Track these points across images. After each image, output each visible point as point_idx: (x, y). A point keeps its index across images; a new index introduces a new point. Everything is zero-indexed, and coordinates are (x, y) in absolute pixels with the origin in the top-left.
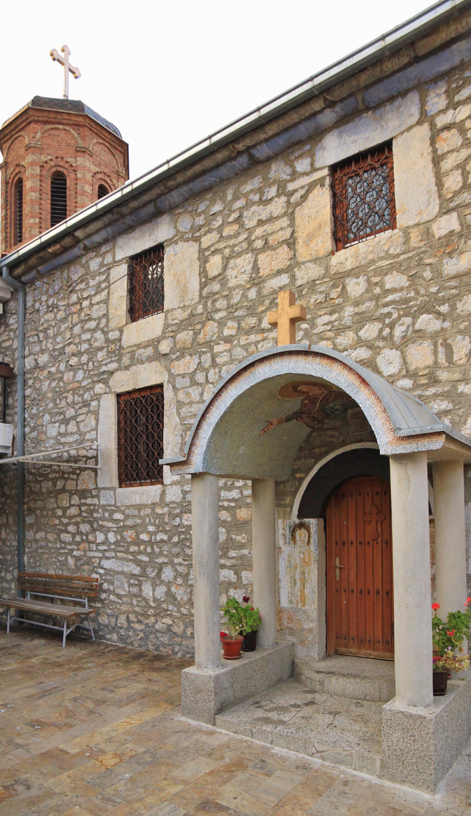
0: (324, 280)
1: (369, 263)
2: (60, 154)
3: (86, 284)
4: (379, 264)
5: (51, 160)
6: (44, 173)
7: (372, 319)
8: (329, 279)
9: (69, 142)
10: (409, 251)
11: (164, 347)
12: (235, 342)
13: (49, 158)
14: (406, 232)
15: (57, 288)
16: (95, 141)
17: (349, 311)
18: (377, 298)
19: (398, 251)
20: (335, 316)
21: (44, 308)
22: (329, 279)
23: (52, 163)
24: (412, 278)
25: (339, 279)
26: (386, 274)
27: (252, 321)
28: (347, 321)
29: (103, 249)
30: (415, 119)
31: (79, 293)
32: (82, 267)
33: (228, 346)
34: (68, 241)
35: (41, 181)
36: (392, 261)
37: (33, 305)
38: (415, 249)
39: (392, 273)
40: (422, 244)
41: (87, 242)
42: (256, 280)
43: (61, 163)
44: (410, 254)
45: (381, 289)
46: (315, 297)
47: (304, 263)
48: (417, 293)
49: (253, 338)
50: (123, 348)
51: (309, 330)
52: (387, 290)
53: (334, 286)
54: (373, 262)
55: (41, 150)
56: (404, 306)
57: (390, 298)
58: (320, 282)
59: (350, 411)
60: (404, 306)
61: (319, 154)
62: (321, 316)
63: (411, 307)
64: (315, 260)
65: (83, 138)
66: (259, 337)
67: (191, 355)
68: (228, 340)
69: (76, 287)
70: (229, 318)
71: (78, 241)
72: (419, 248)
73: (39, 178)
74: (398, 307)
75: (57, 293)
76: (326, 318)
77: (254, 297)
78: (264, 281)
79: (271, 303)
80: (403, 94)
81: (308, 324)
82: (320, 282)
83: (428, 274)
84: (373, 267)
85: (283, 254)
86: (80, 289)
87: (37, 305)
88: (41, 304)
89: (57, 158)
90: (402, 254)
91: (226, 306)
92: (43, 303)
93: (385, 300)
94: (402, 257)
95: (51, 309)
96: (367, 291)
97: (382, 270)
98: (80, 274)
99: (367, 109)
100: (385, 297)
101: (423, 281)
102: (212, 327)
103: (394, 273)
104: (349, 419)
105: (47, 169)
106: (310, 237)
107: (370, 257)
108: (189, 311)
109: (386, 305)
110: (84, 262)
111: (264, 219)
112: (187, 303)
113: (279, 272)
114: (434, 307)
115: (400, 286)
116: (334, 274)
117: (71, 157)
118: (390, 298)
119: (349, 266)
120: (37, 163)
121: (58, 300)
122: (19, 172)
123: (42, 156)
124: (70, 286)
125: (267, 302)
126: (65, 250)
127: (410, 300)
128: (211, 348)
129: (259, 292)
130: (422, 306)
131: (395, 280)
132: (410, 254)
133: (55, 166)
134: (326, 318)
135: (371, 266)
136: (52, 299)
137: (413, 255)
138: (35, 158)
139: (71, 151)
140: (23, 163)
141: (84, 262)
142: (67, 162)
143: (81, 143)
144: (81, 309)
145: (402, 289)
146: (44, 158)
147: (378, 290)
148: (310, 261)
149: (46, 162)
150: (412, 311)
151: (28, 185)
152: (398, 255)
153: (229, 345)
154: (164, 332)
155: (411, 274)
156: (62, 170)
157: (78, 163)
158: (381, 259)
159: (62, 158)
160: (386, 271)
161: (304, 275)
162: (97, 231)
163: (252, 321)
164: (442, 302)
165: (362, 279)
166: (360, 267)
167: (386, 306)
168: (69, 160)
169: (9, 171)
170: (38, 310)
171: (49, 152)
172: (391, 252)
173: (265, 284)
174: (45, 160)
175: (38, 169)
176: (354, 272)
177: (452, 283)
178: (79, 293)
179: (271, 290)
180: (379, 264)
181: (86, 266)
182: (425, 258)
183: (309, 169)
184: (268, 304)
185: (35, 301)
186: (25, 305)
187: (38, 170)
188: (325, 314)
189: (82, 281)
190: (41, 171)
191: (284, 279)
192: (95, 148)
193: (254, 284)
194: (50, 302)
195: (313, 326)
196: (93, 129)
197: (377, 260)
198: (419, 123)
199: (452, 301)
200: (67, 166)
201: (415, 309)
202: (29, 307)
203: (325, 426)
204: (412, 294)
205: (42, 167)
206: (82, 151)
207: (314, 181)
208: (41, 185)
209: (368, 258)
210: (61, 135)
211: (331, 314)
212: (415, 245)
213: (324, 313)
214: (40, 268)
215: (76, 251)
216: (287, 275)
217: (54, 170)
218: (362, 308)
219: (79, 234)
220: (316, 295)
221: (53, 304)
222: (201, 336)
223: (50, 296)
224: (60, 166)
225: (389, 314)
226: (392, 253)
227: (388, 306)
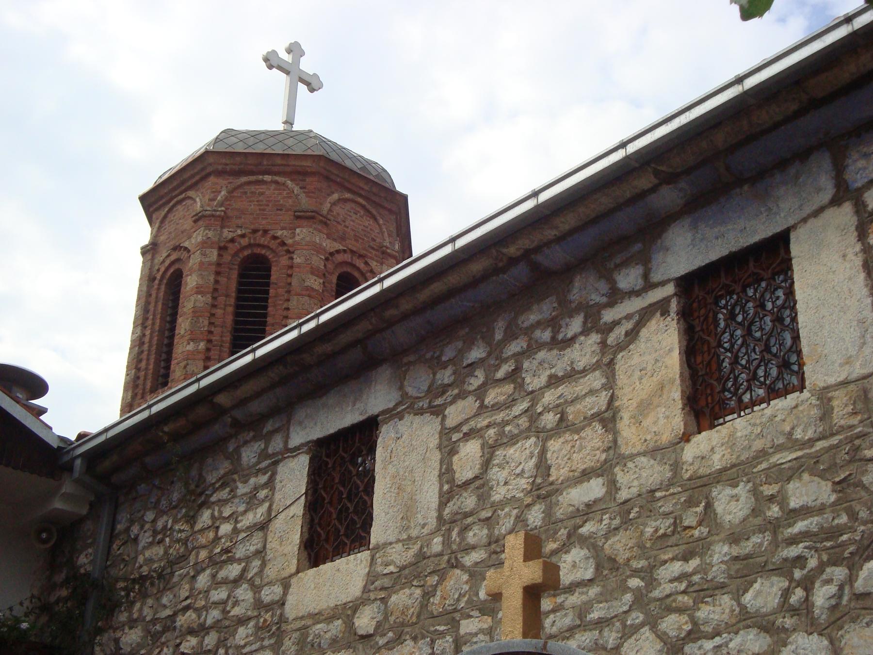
0: (672, 491)
1: (755, 458)
2: (263, 223)
3: (232, 491)
4: (774, 459)
5: (243, 236)
6: (227, 258)
7: (765, 570)
8: (680, 489)
9: (281, 202)
10: (832, 435)
11: (365, 621)
13: (239, 232)
14: (824, 395)
15: (176, 496)
16: (336, 196)
17: (721, 551)
18: (774, 526)
19: (810, 434)
20: (694, 563)
21: (147, 534)
22: (680, 489)
23: (244, 242)
25: (699, 488)
26: (789, 480)
28: (717, 572)
29: (269, 426)
30: (826, 196)
31: (217, 508)
32: (227, 458)
34: (202, 411)
35: (218, 273)
36: (799, 453)
37: (127, 530)
38: (842, 429)
39: (800, 478)
40: (855, 421)
41: (238, 414)
43: (262, 241)
44: (834, 440)
45: (780, 508)
46: (654, 524)
47: (632, 457)
48: (853, 516)
51: (644, 592)
52: (794, 511)
53: (690, 503)
54: (763, 454)
55: (224, 220)
56: (828, 544)
57: (800, 526)
58: (664, 493)
60: (828, 544)
61: (658, 258)
62: (665, 562)
63: (843, 545)
64: (654, 452)
67: (415, 639)
69: (211, 495)
70: (490, 563)
71: (221, 412)
72: (851, 427)
73: (213, 268)
74: (818, 545)
75: (175, 507)
76: (677, 567)
77: (538, 523)
78: (557, 490)
79: (569, 536)
80: (803, 155)
81: (642, 579)
82: (664, 493)
84: (764, 466)
85: (594, 438)
86: (219, 501)
87: (135, 529)
88: (142, 527)
90: (819, 439)
91: (485, 540)
92: (147, 526)
93: (789, 530)
94: (820, 445)
95: (159, 537)
96: (755, 512)
97: (781, 471)
98: (222, 472)
99: (739, 182)
100: (790, 525)
101: (863, 493)
102: (457, 580)
103: (806, 476)
105: (232, 252)
106: (644, 407)
107: (758, 445)
108: (416, 547)
109: (793, 541)
110: (231, 450)
111: (560, 374)
112: (414, 533)
113: (586, 475)
115: (819, 502)
116: (690, 479)
117: (282, 229)
118: (800, 526)
119: (717, 462)
120: (213, 243)
121: (175, 521)
122: (178, 260)
123: (225, 231)
124: (201, 494)
125: (563, 533)
126: (197, 427)
127: (839, 531)
128: (455, 625)
129: (548, 513)
130: (866, 542)
131: (806, 491)
132: (834, 440)
133: (250, 246)
134: (677, 567)
135: (761, 463)
136: (165, 518)
137: (840, 441)
138: (210, 234)
140: (186, 244)
141: (231, 450)
142: (275, 238)
143: (305, 202)
144: (217, 539)
145: (821, 509)
146: (227, 234)
147: (774, 511)
148: (644, 454)
149: (232, 240)
150: (846, 555)
151: (191, 281)
152: (812, 442)
153: (490, 620)
154: (365, 590)
155: (837, 479)
157: (297, 238)
158: (779, 448)
159: (265, 232)
160: (790, 473)
161: (634, 479)
162: (258, 395)
165: (742, 490)
166: (739, 464)
167: (791, 544)
169: (159, 259)
170: (136, 540)
171: (240, 222)
172: (798, 434)
173: (560, 498)
174: (231, 235)
176: (728, 475)
178: (217, 508)
179: (571, 509)
181: (235, 457)
182: (863, 446)
183: (640, 283)
184: (565, 537)
185: (132, 522)
186: (113, 528)
187: (213, 255)
188: (672, 559)
189: (223, 486)
190: (220, 255)
191: (595, 489)
192: (337, 209)
193: (538, 497)
194: (160, 524)
195: (651, 582)
196: (333, 177)
197: (771, 450)
198: (836, 201)
200: (273, 244)
201: (852, 548)
202: (120, 533)
204: (844, 519)
205: (222, 249)
206: (303, 217)
207: (651, 305)
208: (217, 282)
209: (754, 449)
211: (686, 558)
212: (842, 422)
213: (671, 556)
214: (148, 460)
215: (217, 429)
216: (600, 480)
218: (747, 547)
219: (222, 399)
220: (656, 521)
221: (165, 527)
222: (436, 600)
223: (163, 513)
224: (259, 245)
225: (800, 561)
226: (799, 436)
227: (798, 543)
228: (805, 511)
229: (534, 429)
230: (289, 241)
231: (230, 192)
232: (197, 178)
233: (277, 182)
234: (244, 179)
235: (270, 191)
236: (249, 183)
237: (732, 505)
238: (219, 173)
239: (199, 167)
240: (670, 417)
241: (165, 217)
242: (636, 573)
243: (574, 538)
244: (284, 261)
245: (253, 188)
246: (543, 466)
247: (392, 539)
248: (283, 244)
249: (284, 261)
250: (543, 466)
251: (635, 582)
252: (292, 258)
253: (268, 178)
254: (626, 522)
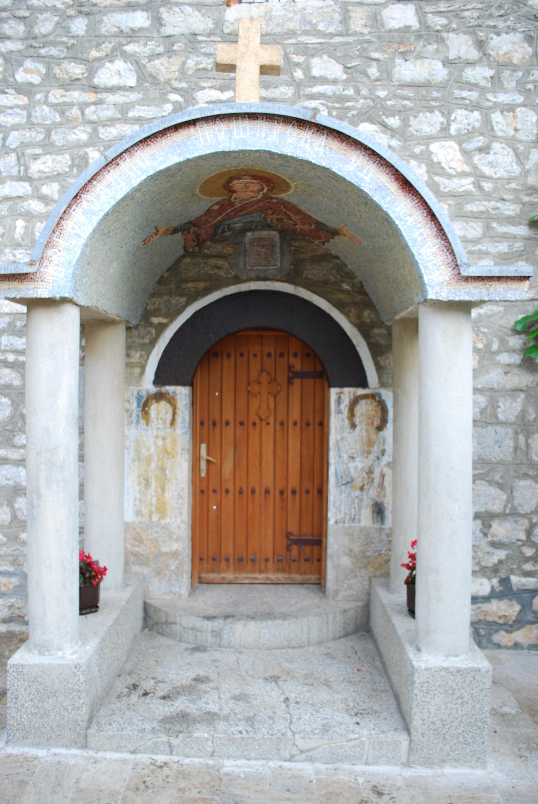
0: (212, 38)
1: (286, 34)
4: (303, 39)
8: (220, 39)
10: (348, 35)
12: (39, 96)
19: (331, 30)
22: (220, 39)
26: (313, 56)
27: (77, 70)
33: (23, 100)
36: (322, 40)
38: (355, 34)
39: (321, 57)
40: (366, 31)
44: (350, 39)
45: (304, 73)
46: (196, 59)
48: (358, 91)
49: (76, 95)
51: (183, 105)
52: (314, 78)
56: (337, 105)
58: (205, 39)
59: (249, 234)
60: (337, 105)
62: (204, 88)
63: (348, 109)
66: (90, 97)
68: (25, 90)
70: (27, 54)
72: (362, 34)
74: (329, 104)
77: (82, 33)
78: (100, 12)
79: (113, 50)
81: (182, 96)
82: (205, 39)
83: (373, 71)
84: (293, 41)
90: (338, 35)
91: (21, 34)
93: (309, 89)
94: (337, 39)
97: (307, 48)
100: (311, 87)
101: (365, 79)
103: (325, 57)
104: (248, 246)
109: (312, 97)
114: (380, 116)
115: (333, 77)
116: (229, 34)
125: (107, 47)
127: (348, 99)
130: (364, 111)
132: (350, 39)
135: (290, 38)
137: (354, 41)
145: (335, 82)
148: (190, 5)
150: (349, 115)
152: (332, 35)
153: (26, 99)
155: (349, 65)
158: (306, 33)
160: (314, 52)
163: (77, 70)
164: (392, 112)
166: (272, 35)
167: (311, 99)
172: (321, 27)
177: (407, 92)
179: (115, 29)
182: (370, 49)
184: (109, 50)
188: (211, 87)
193: (80, 12)
197: (299, 32)
199: (404, 113)
201: (355, 112)
203: (206, 251)
204: (350, 92)
209: (286, 27)
212: (357, 29)
213: (210, 85)
220: (198, 56)
226: (321, 29)
227: (314, 99)
228: (323, 80)
242: (176, 90)
243: (116, 53)
251: (174, 97)
254: (170, 52)
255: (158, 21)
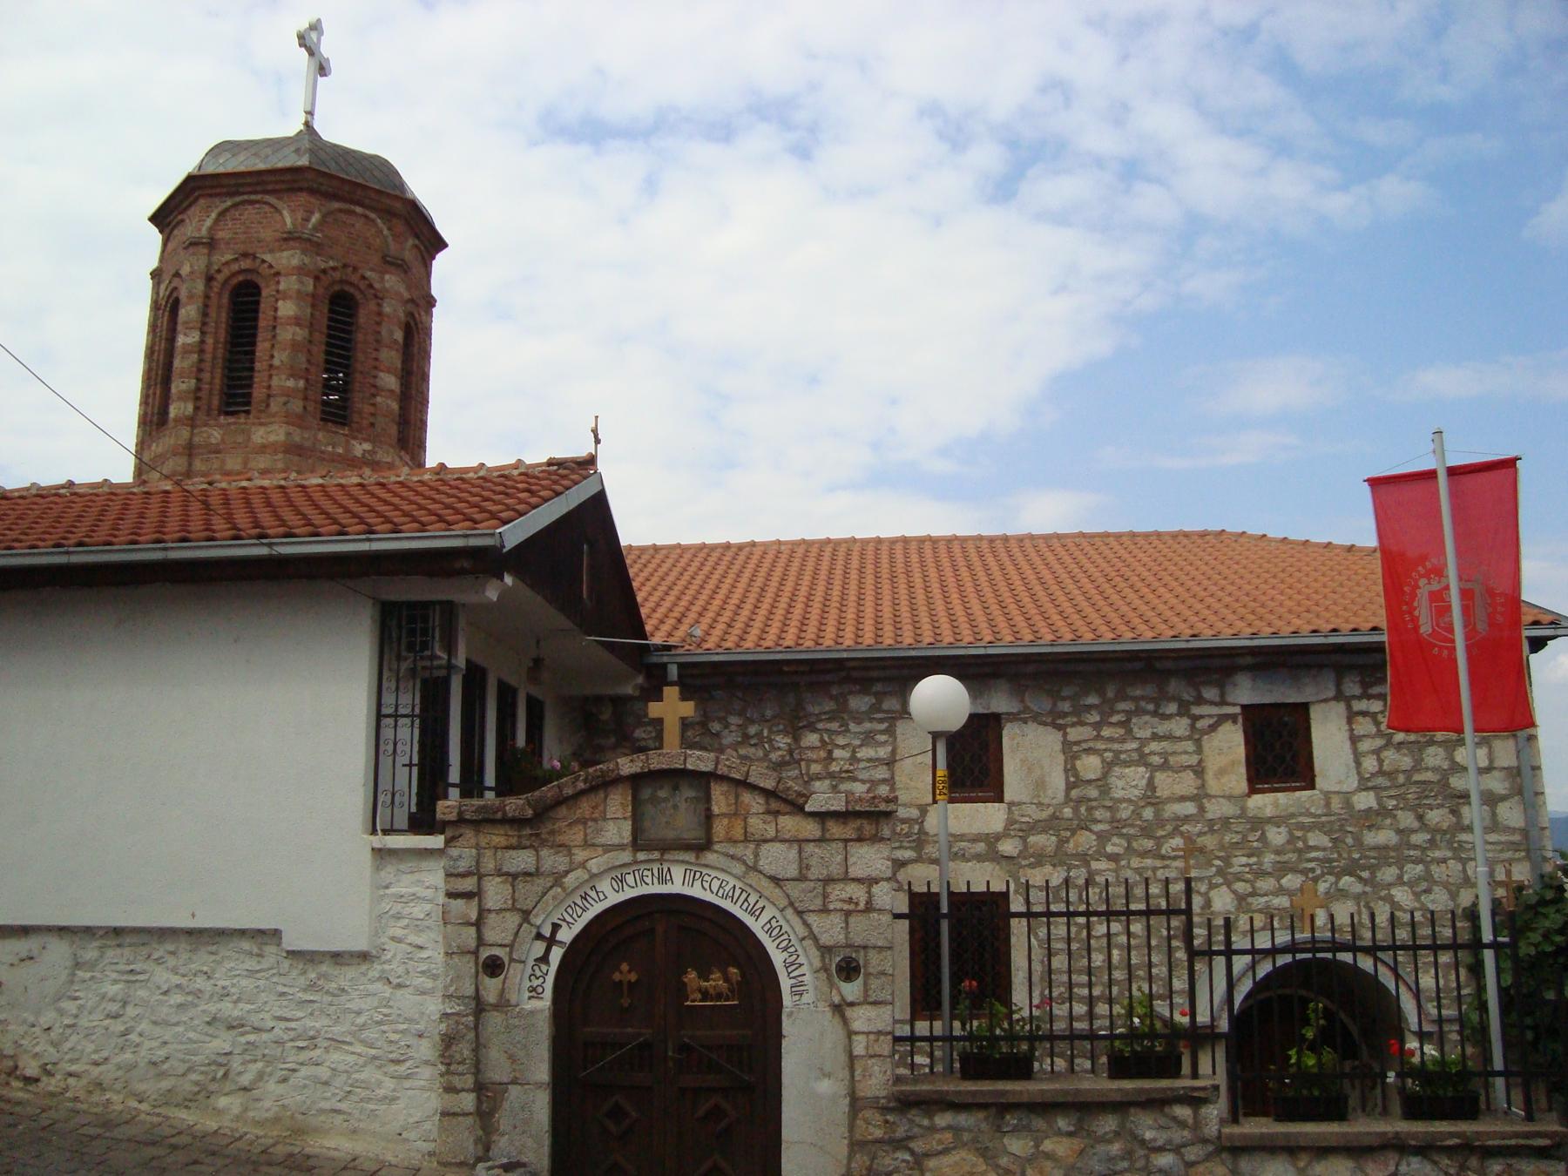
5: (334, 269)
11: (1008, 847)
12: (1123, 863)
13: (331, 263)
17: (1269, 859)
20: (1254, 860)
23: (337, 275)
24: (1334, 841)
25: (1258, 823)
27: (1149, 844)
33: (1112, 865)
42: (1150, 796)
49: (1148, 862)
50: (927, 834)
53: (1253, 830)
54: (1293, 815)
64: (1229, 797)
65: (396, 236)
66: (1158, 863)
67: (1054, 866)
68: (1113, 858)
76: (1244, 860)
89: (345, 266)
96: (1288, 842)
107: (1292, 810)
108: (1051, 810)
112: (1046, 801)
113: (1183, 799)
117: (372, 270)
119: (1269, 812)
125: (1169, 828)
128: (1087, 864)
131: (1315, 838)
133: (341, 281)
134: (1244, 860)
138: (307, 260)
139: (375, 259)
142: (363, 278)
154: (1006, 828)
156: (352, 290)
158: (1301, 814)
159: (355, 269)
161: (1215, 809)
163: (1149, 844)
165: (1283, 829)
168: (368, 274)
175: (311, 282)
176: (1276, 821)
180: (1301, 819)
195: (1229, 864)
200: (363, 285)
205: (317, 278)
210: (357, 226)
217: (337, 288)
222: (1071, 845)
224: (351, 284)
229: (1142, 760)
230: (377, 286)
231: (324, 216)
232: (283, 186)
233: (366, 217)
234: (336, 205)
235: (359, 224)
236: (340, 211)
237: (1277, 836)
238: (312, 191)
239: (288, 177)
240: (1238, 780)
241: (227, 210)
243: (1176, 831)
244: (372, 305)
245: (344, 217)
246: (1151, 785)
247: (1027, 800)
248: (371, 286)
249: (372, 305)
250: (1151, 785)
252: (379, 305)
253: (359, 210)
254: (1212, 831)
255: (1202, 809)
